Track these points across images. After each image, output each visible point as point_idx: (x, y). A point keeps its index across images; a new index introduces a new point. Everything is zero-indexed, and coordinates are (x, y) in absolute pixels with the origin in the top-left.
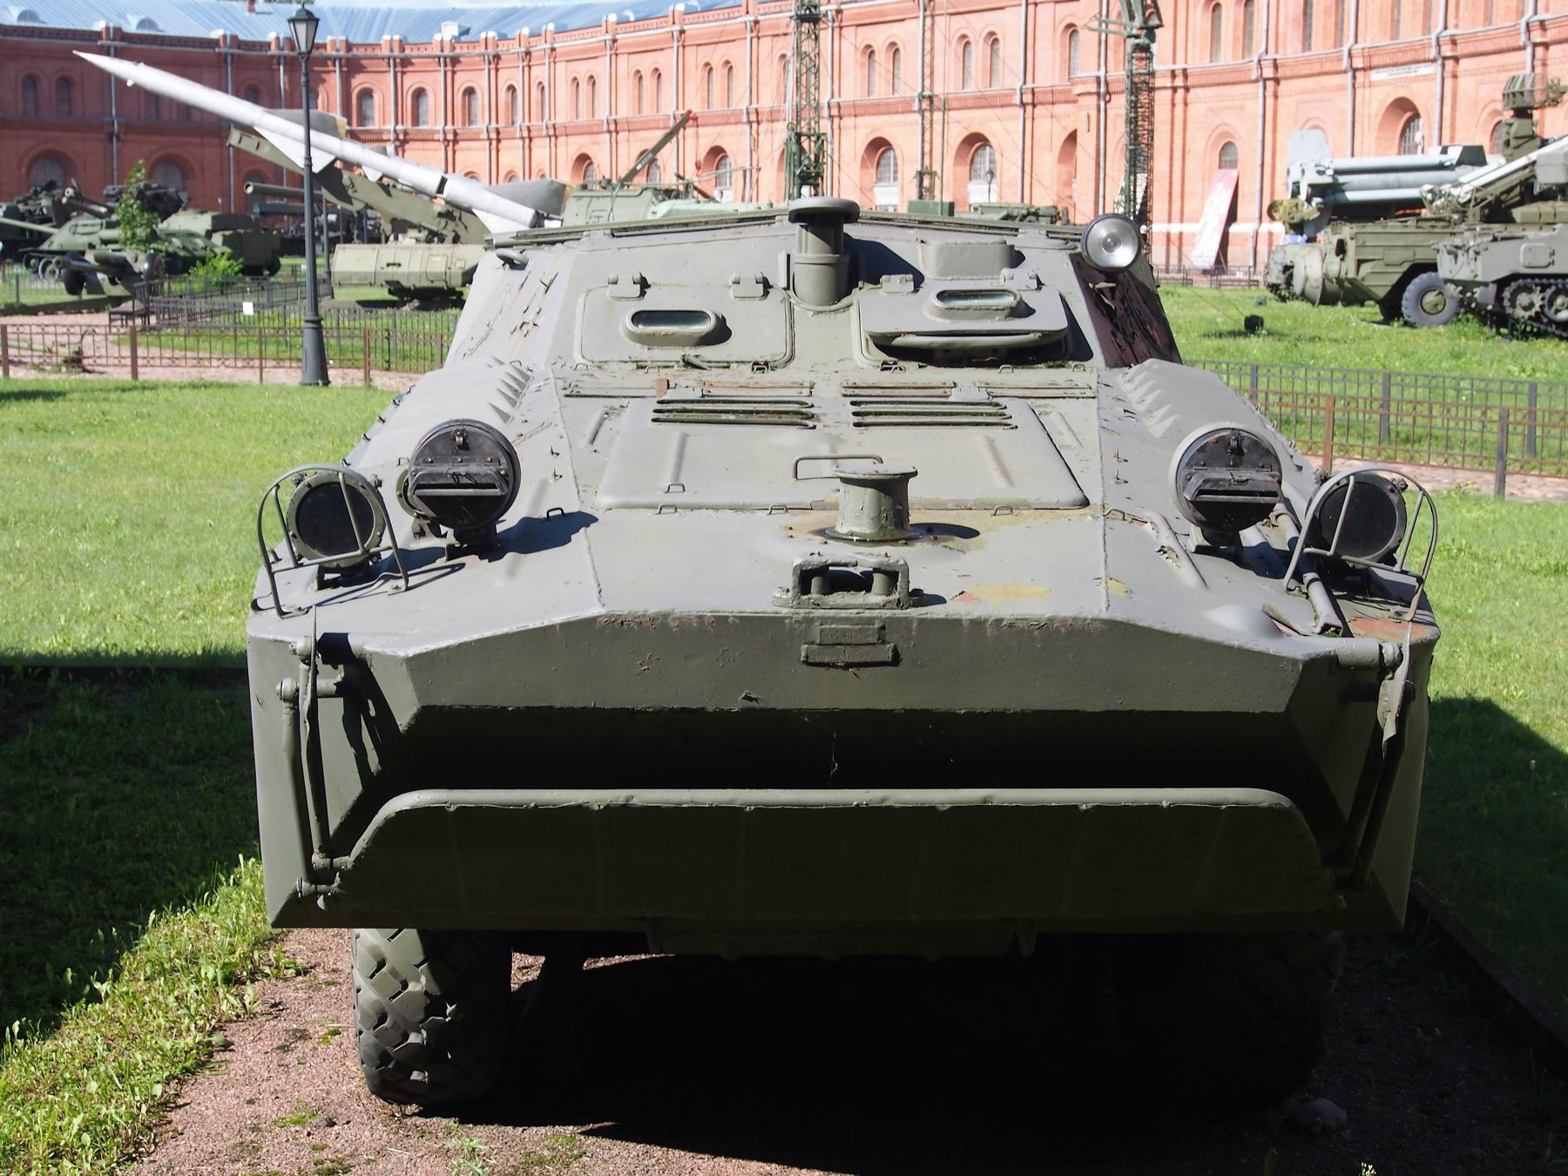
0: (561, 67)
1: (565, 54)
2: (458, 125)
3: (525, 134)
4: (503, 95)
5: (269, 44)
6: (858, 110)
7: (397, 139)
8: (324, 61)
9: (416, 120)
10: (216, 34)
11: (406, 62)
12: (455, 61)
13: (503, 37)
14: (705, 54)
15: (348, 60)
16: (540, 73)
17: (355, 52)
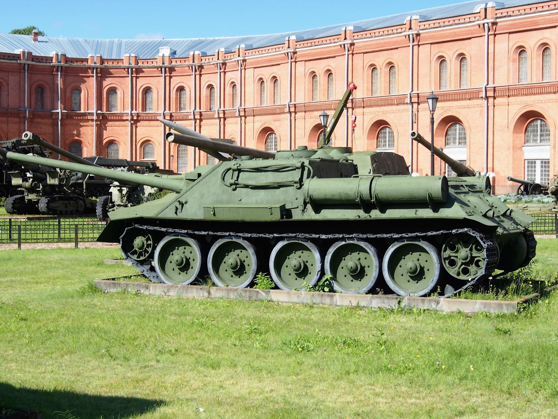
0: (249, 73)
1: (252, 63)
2: (173, 110)
3: (221, 115)
4: (205, 92)
5: (51, 59)
6: (510, 92)
7: (132, 119)
8: (85, 70)
9: (144, 107)
10: (18, 51)
11: (139, 71)
12: (172, 69)
13: (204, 55)
14: (370, 59)
15: (101, 68)
16: (233, 76)
17: (106, 64)
